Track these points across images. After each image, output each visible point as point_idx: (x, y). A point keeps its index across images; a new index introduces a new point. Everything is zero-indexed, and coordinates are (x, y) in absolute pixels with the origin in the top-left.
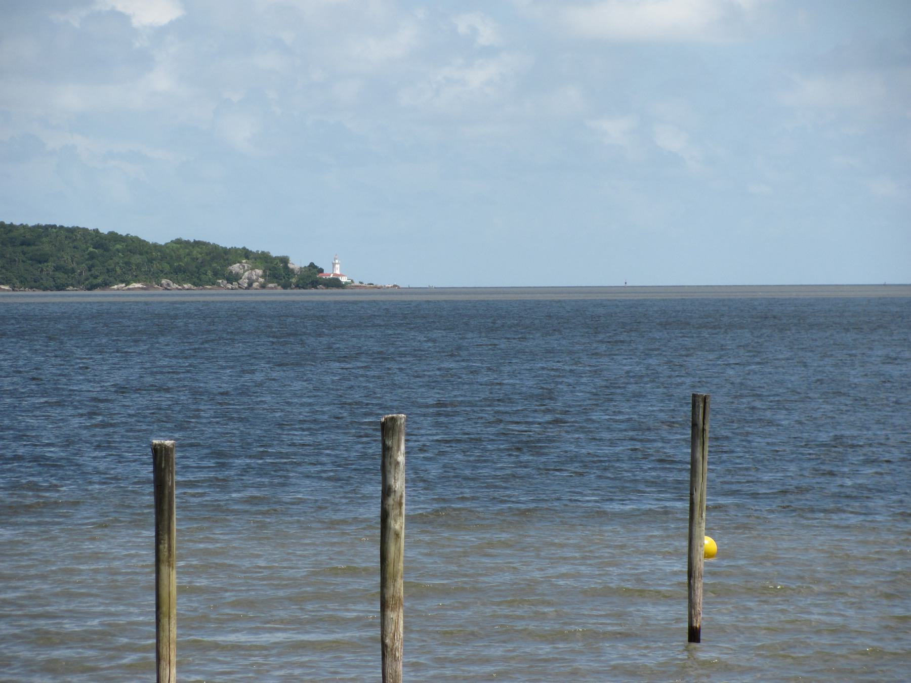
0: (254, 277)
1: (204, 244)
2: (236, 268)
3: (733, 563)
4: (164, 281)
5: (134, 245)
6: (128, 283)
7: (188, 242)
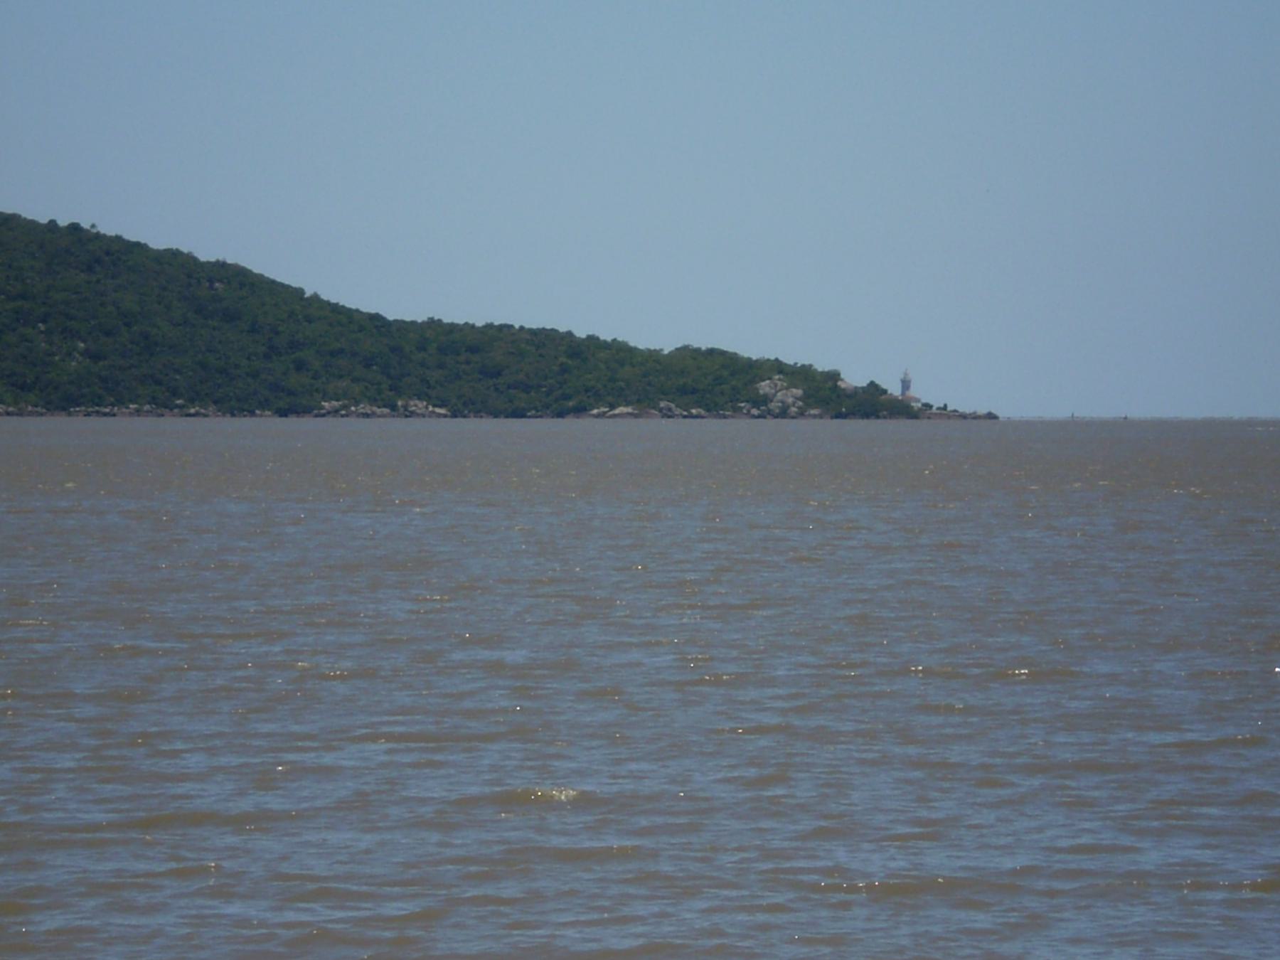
0: (790, 400)
1: (723, 353)
2: (764, 387)
3: (753, 826)
4: (662, 404)
5: (620, 353)
6: (612, 407)
7: (698, 351)
